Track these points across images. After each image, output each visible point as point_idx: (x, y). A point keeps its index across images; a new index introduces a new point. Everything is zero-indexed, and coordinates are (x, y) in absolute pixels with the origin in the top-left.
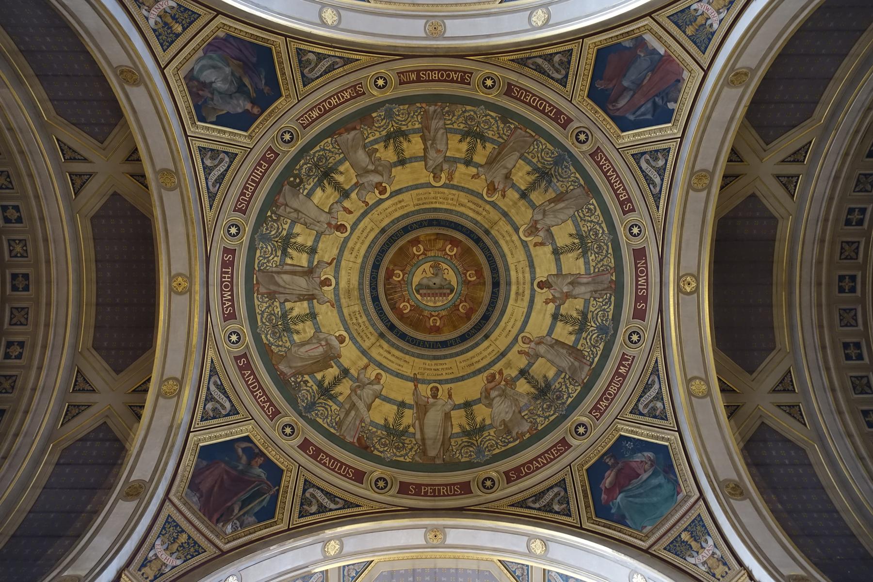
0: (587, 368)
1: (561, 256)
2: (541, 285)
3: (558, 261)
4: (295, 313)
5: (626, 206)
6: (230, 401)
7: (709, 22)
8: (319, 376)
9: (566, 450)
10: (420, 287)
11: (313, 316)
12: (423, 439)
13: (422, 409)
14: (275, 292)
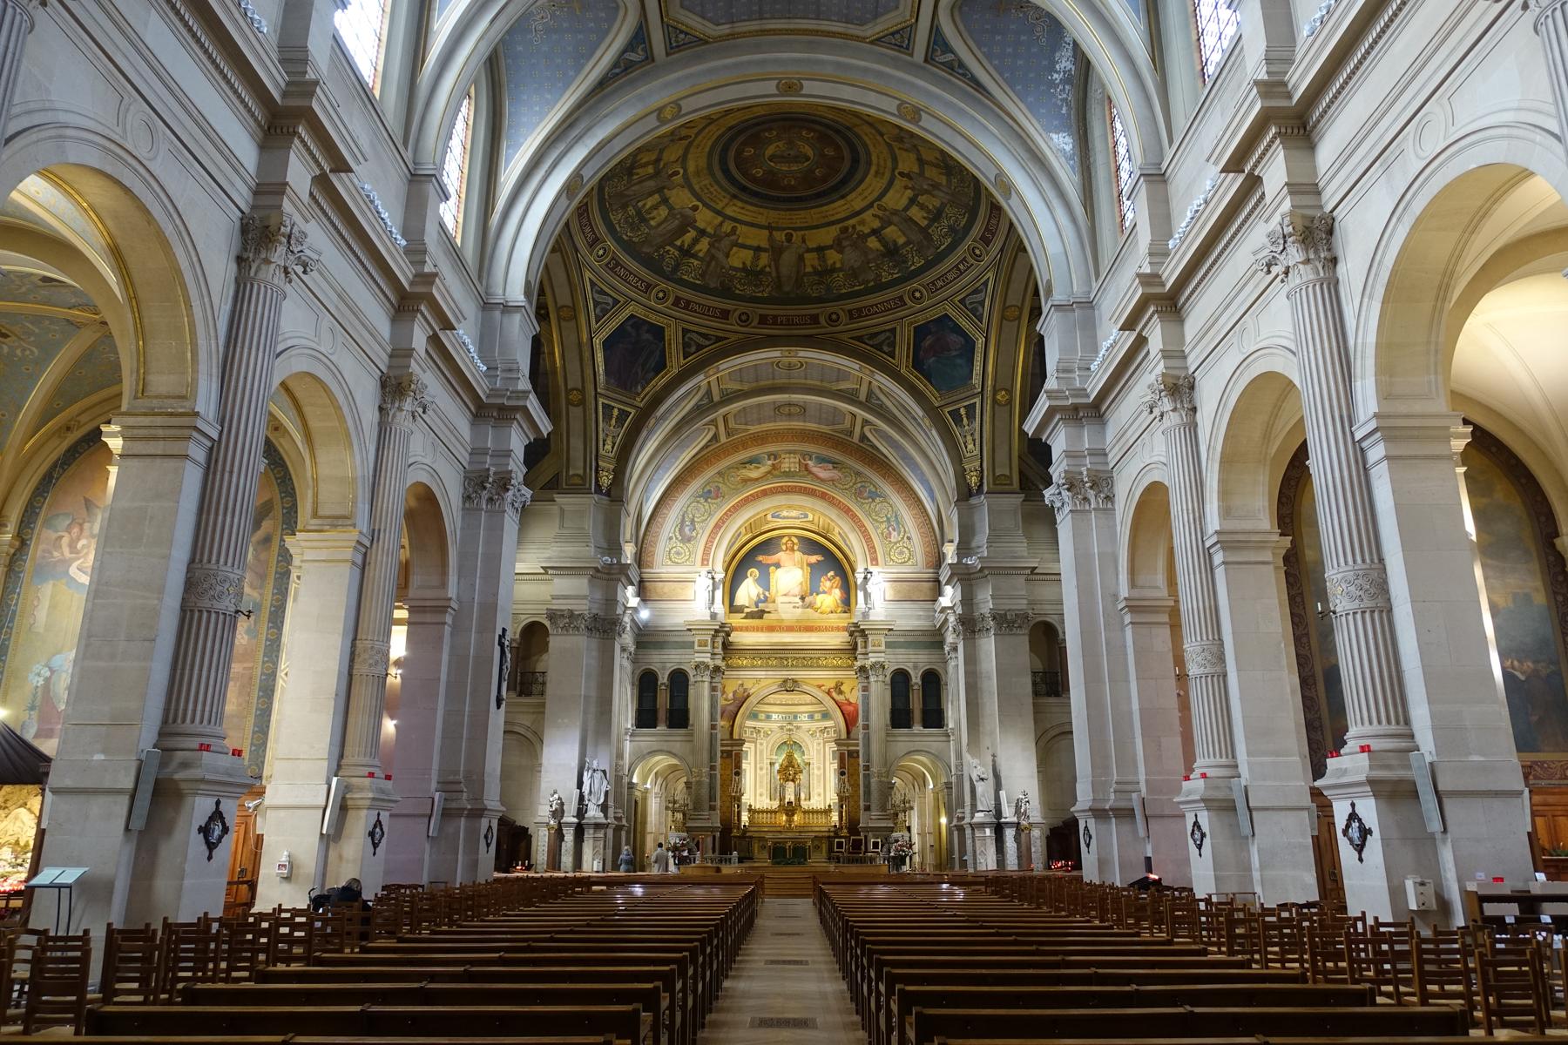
8: (678, 243)
11: (665, 201)
12: (778, 277)
13: (777, 251)
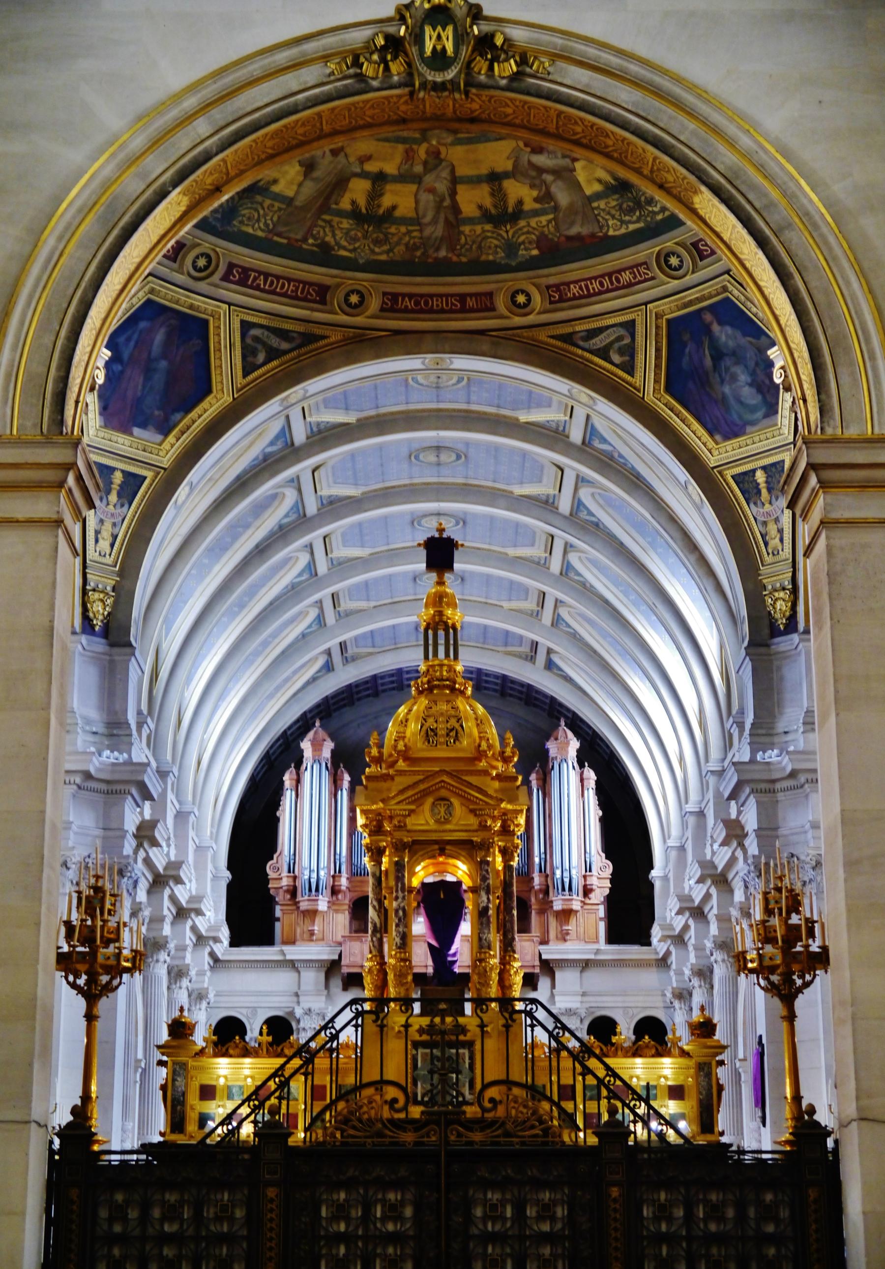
7: (105, 501)
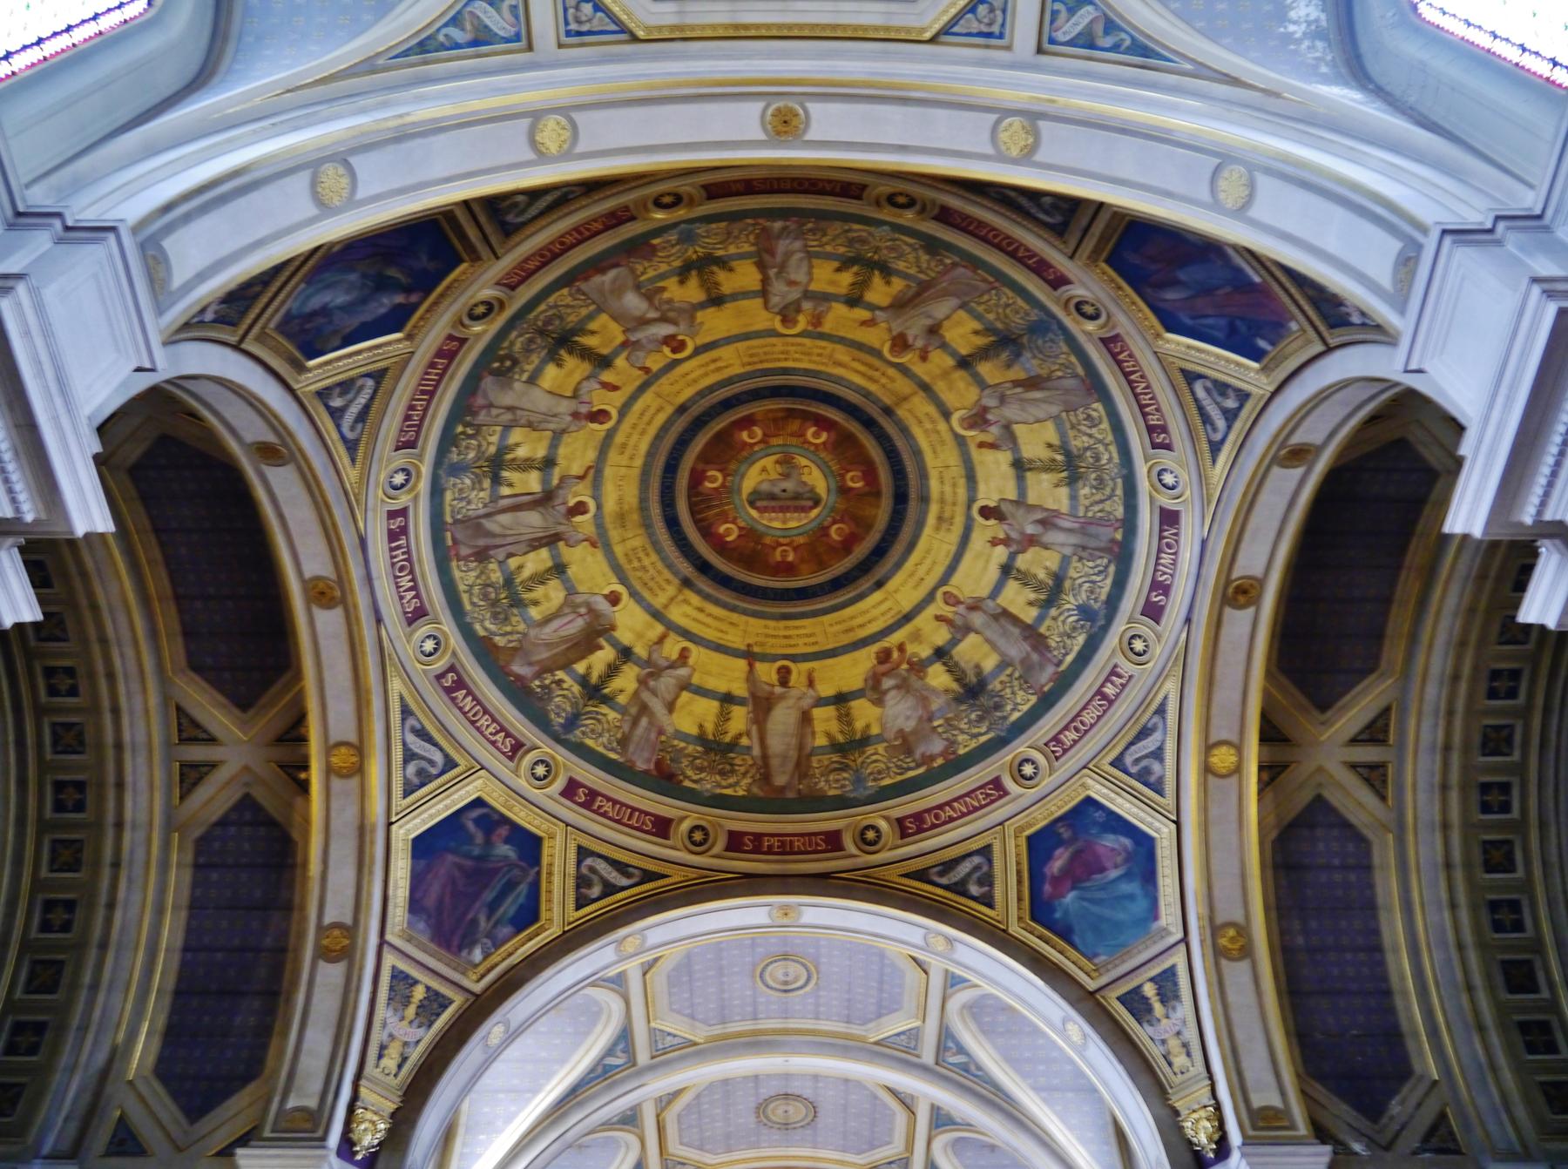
0: (1050, 670)
1: (1029, 474)
2: (986, 512)
3: (1020, 479)
4: (526, 573)
5: (1158, 436)
6: (441, 749)
8: (580, 667)
9: (1000, 797)
10: (755, 498)
11: (559, 569)
12: (765, 757)
13: (762, 705)
14: (488, 548)
